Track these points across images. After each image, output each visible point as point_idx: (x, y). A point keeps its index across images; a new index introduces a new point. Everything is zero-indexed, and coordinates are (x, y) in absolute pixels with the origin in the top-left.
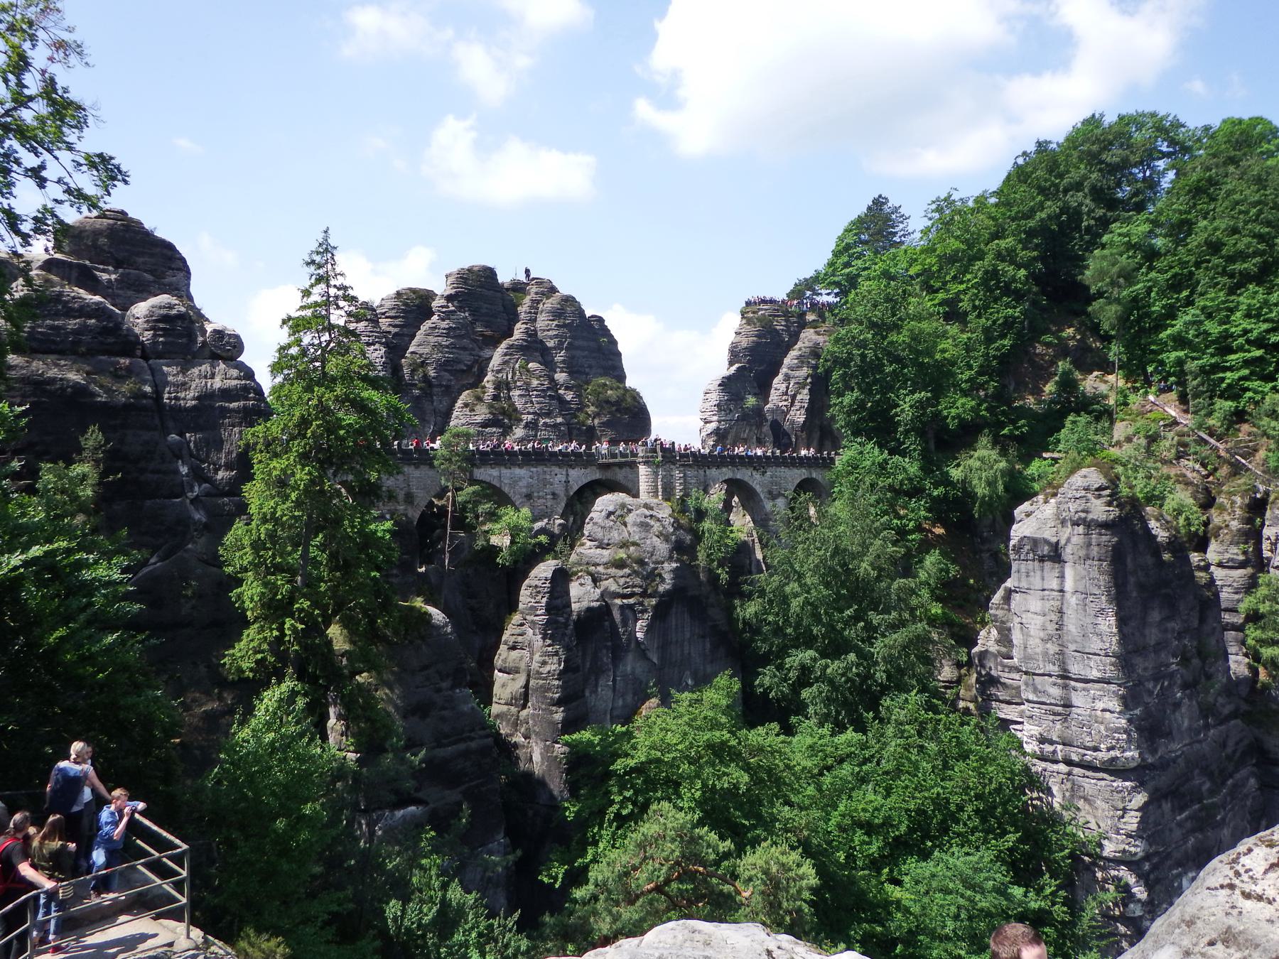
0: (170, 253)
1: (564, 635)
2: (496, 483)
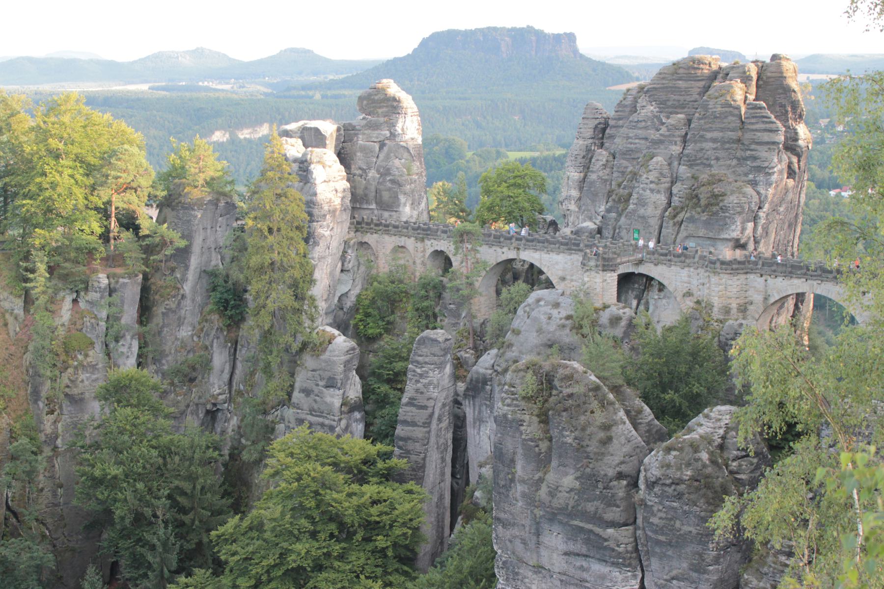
0: (395, 104)
1: (417, 381)
2: (537, 264)
